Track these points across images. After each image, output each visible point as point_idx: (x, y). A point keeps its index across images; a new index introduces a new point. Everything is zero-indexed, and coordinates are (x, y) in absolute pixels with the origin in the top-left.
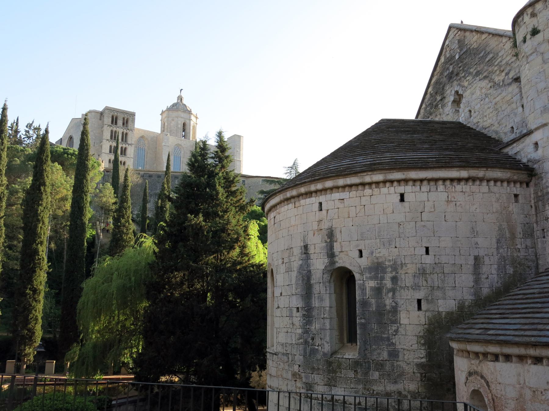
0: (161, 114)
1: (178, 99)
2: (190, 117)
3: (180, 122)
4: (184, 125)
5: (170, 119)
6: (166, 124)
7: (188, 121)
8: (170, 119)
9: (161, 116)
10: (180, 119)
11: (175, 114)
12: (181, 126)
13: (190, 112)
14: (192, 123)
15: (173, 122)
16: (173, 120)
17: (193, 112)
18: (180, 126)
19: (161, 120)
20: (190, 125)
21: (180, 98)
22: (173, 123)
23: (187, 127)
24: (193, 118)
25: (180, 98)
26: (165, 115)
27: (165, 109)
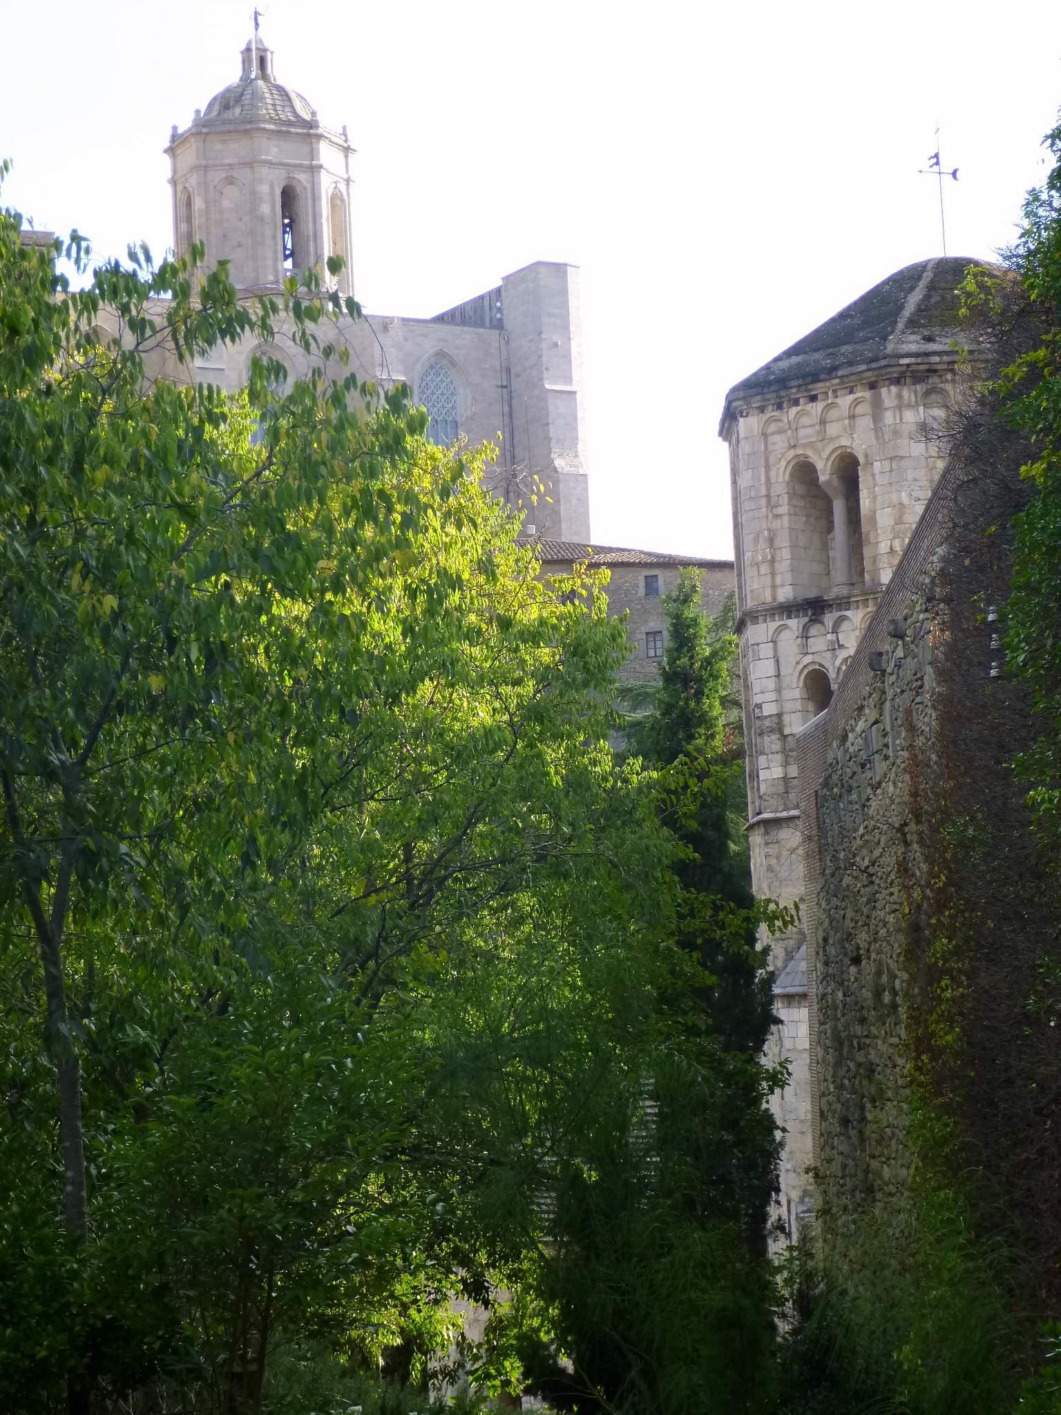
0: (171, 151)
1: (246, 61)
2: (313, 154)
3: (264, 189)
4: (288, 198)
5: (217, 176)
6: (198, 204)
7: (302, 177)
8: (217, 176)
9: (167, 161)
10: (264, 171)
11: (233, 150)
12: (270, 207)
13: (305, 131)
14: (326, 184)
15: (231, 192)
16: (230, 181)
17: (327, 123)
18: (265, 209)
19: (173, 182)
20: (315, 199)
21: (257, 59)
22: (230, 198)
23: (303, 206)
24: (327, 155)
25: (257, 59)
26: (189, 156)
27: (185, 125)
